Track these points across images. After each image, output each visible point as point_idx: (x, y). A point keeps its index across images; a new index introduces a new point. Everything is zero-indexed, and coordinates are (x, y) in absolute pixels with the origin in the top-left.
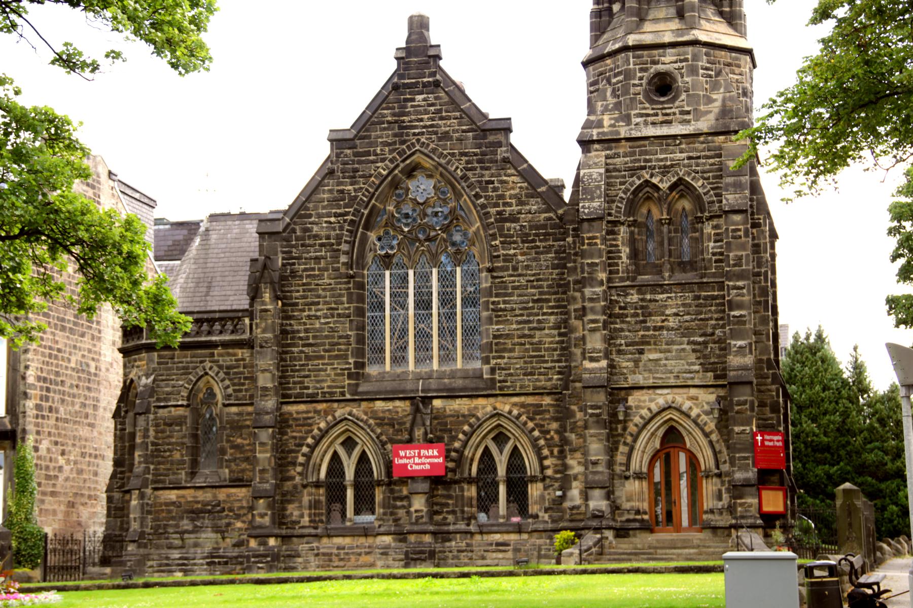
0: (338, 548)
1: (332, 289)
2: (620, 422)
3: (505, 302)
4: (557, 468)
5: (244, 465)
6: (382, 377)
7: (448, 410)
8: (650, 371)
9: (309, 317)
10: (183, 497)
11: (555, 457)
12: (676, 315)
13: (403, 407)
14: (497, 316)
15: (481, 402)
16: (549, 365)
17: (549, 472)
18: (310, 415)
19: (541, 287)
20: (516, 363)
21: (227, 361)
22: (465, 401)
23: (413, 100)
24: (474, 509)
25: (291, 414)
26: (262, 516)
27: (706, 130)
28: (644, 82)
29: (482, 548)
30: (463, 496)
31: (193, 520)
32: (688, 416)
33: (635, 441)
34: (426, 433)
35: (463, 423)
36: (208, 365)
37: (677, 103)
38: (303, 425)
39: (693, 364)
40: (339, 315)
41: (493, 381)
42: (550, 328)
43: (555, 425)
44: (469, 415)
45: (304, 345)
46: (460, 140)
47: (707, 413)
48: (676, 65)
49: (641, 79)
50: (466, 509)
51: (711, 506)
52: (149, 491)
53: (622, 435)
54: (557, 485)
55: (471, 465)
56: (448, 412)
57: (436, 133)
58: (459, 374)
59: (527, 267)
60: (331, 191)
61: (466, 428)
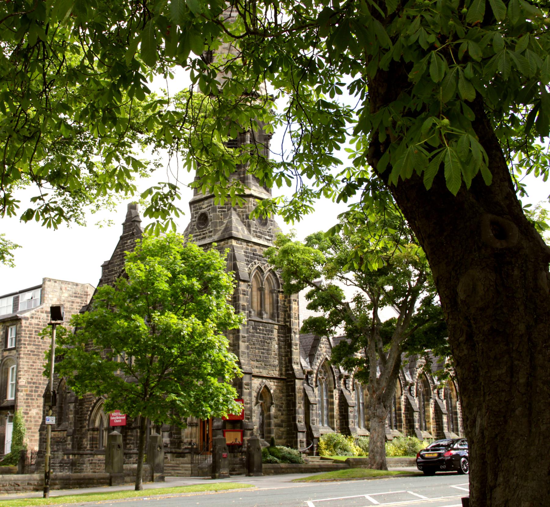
0: (99, 460)
26: (69, 444)
31: (57, 446)
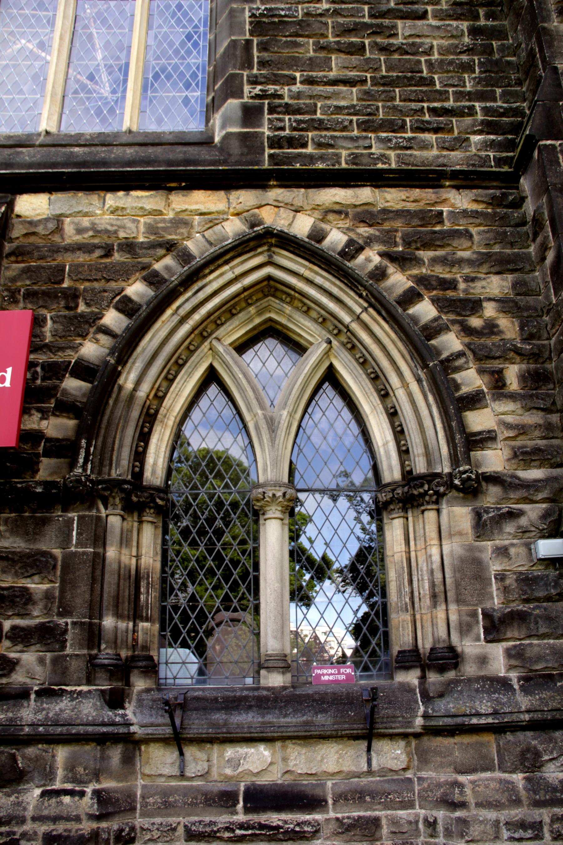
4: (528, 443)
7: (69, 228)
11: (512, 397)
20: (335, 95)
24: (147, 628)
29: (180, 820)
30: (99, 560)
35: (125, 273)
44: (153, 246)
50: (108, 622)
54: (533, 512)
55: (144, 437)
56: (70, 234)
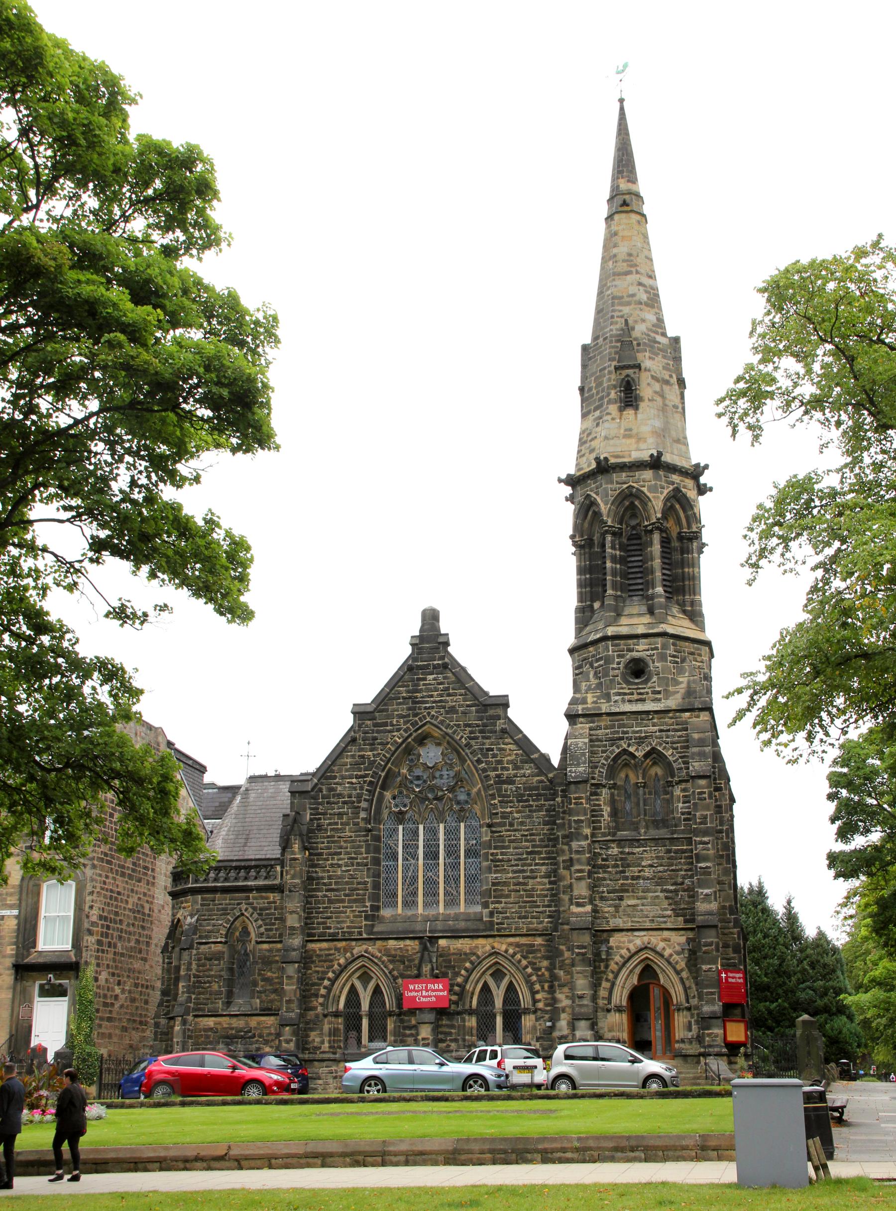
1: (353, 841)
2: (602, 960)
3: (502, 854)
5: (273, 996)
6: (394, 919)
8: (629, 915)
9: (332, 865)
10: (220, 1023)
12: (651, 866)
13: (413, 946)
14: (496, 866)
15: (481, 941)
16: (541, 909)
17: (540, 1005)
18: (332, 952)
19: (534, 840)
21: (260, 903)
22: (467, 941)
23: (425, 679)
24: (474, 1038)
25: (314, 951)
26: (288, 1042)
27: (674, 707)
28: (621, 666)
31: (227, 1044)
32: (662, 956)
33: (616, 977)
34: (432, 969)
35: (465, 961)
36: (244, 906)
37: (649, 685)
38: (325, 961)
39: (666, 909)
40: (358, 864)
41: (491, 923)
42: (541, 877)
43: (545, 963)
45: (327, 890)
46: (464, 713)
47: (678, 953)
48: (648, 653)
49: (619, 663)
51: (682, 1036)
52: (190, 1018)
53: (604, 972)
54: (547, 1016)
56: (452, 951)
57: (444, 707)
58: (462, 917)
59: (522, 823)
60: (353, 756)
61: (468, 965)
